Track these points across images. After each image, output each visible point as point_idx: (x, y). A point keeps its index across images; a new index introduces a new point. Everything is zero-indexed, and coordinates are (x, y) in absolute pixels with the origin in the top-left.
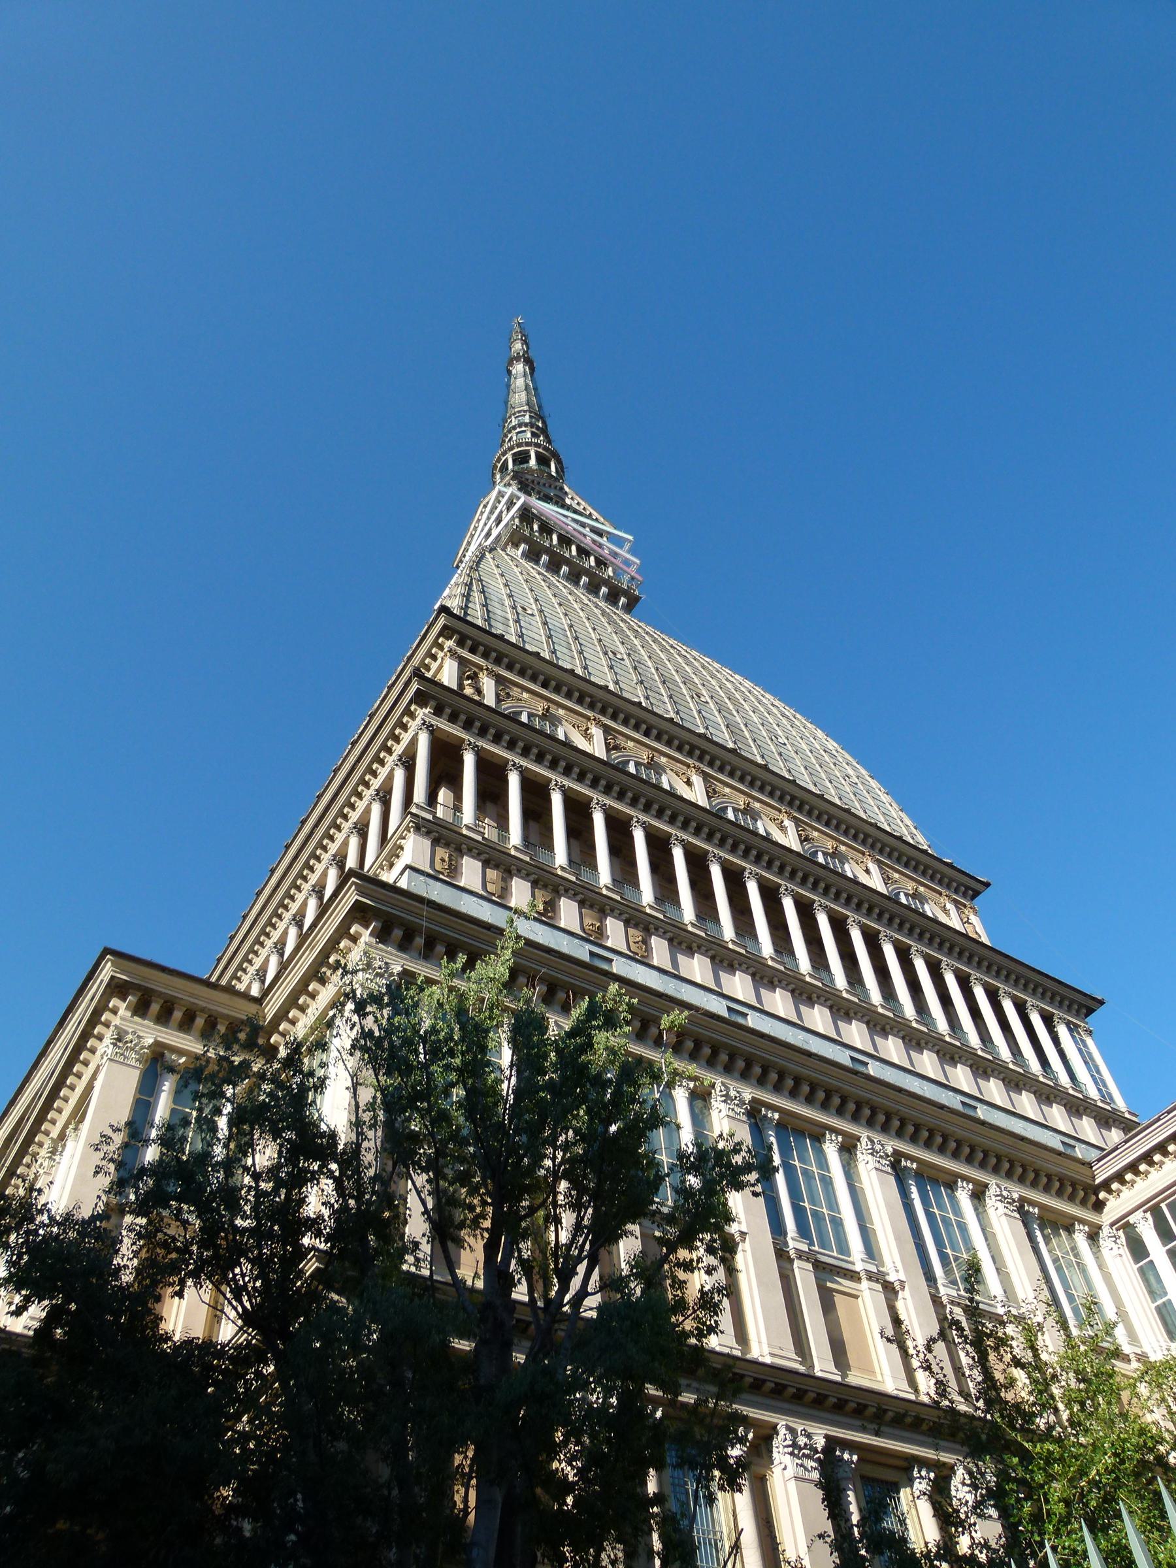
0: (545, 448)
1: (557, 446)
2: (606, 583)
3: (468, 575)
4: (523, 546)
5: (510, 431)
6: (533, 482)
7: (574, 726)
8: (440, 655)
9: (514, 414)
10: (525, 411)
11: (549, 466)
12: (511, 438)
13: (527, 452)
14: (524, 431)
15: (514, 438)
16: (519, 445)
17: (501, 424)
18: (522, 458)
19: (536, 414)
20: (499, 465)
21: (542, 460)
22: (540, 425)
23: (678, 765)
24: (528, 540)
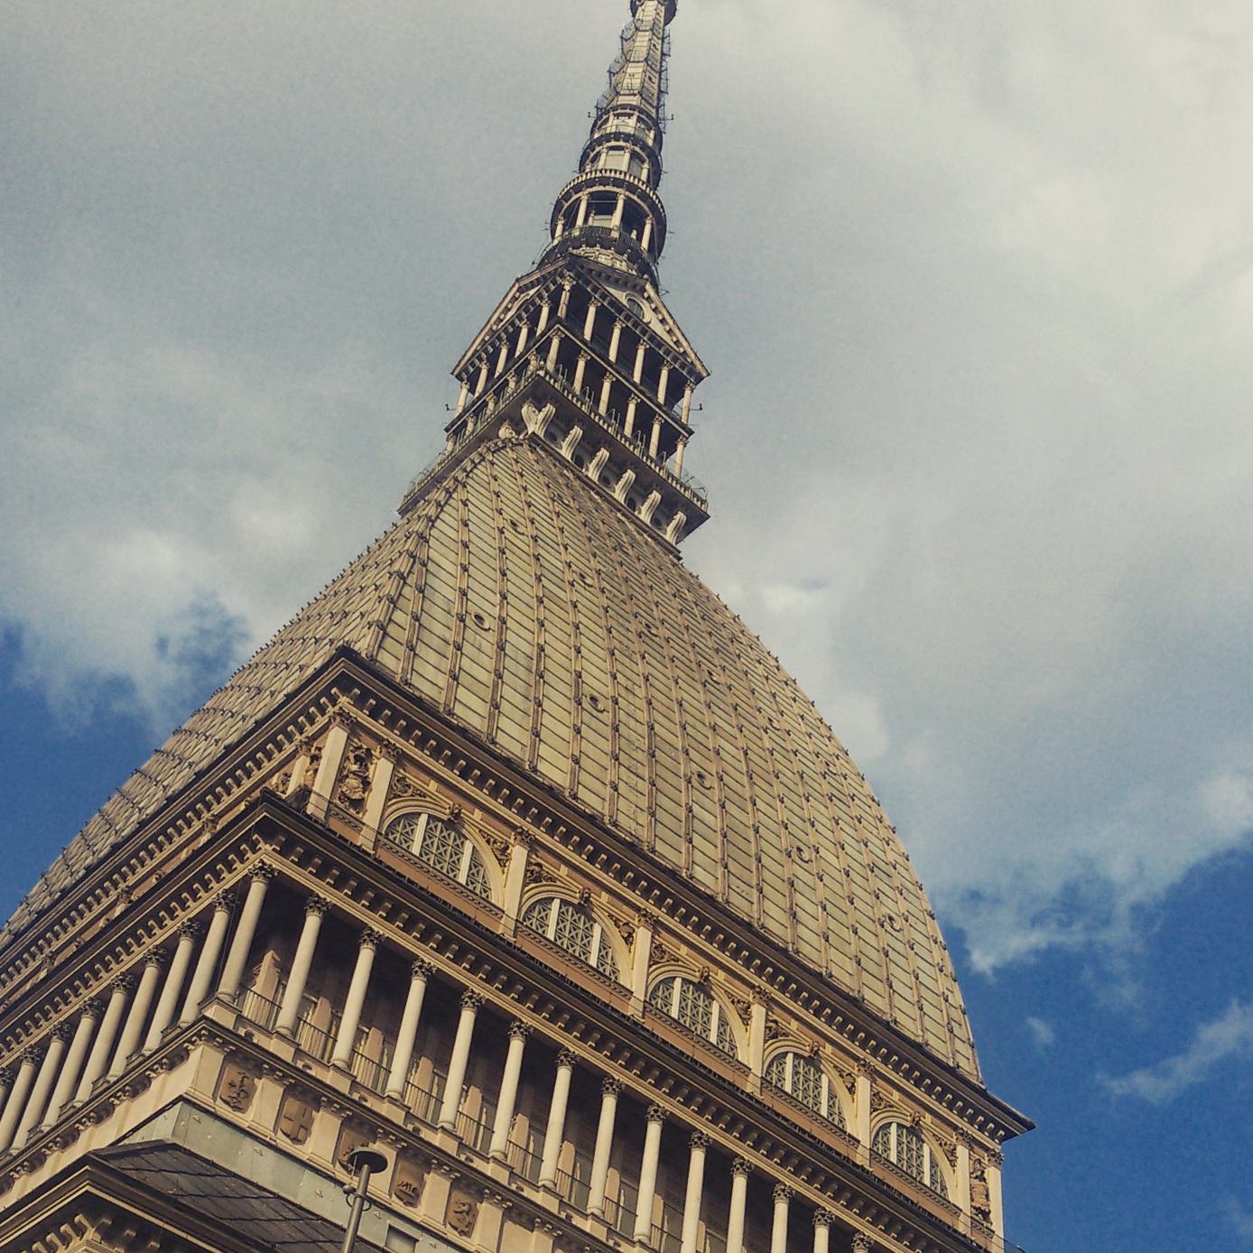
0: (644, 196)
1: (665, 193)
2: (661, 485)
3: (412, 556)
4: (549, 409)
5: (599, 142)
6: (599, 274)
7: (488, 842)
8: (331, 710)
9: (614, 109)
10: (633, 108)
11: (640, 237)
12: (599, 154)
13: (614, 196)
14: (621, 148)
15: (601, 164)
16: (604, 181)
17: (594, 113)
18: (602, 205)
19: (649, 116)
20: (566, 205)
21: (633, 219)
22: (650, 143)
23: (625, 908)
24: (557, 399)
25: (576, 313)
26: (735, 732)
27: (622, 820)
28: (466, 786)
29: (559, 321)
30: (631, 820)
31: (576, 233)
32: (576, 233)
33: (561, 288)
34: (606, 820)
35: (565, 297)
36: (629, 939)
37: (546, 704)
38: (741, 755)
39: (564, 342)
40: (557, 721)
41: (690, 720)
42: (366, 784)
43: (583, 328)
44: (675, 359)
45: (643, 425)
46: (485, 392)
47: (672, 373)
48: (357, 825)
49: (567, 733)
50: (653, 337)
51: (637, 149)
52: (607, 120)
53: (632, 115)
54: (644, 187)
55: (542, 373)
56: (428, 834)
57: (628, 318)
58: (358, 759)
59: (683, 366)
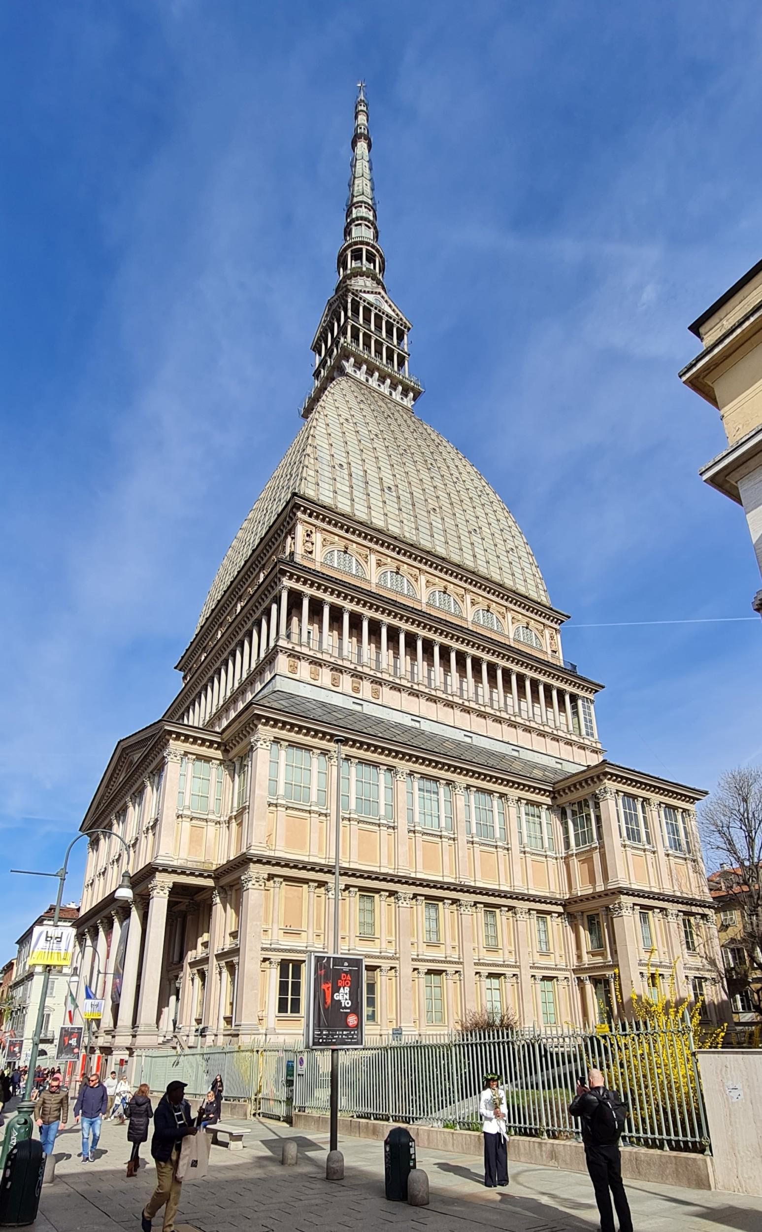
0: (373, 247)
4: (352, 360)
5: (350, 224)
6: (361, 291)
10: (362, 202)
13: (361, 249)
14: (360, 224)
16: (356, 243)
17: (346, 209)
19: (369, 205)
20: (342, 259)
22: (371, 218)
23: (414, 569)
25: (356, 311)
26: (443, 487)
27: (407, 535)
28: (348, 536)
29: (349, 318)
30: (410, 535)
31: (349, 272)
32: (349, 272)
33: (347, 302)
34: (401, 536)
35: (349, 305)
36: (416, 581)
37: (371, 494)
38: (446, 496)
39: (353, 326)
40: (376, 502)
41: (427, 486)
42: (313, 544)
43: (358, 318)
44: (398, 323)
45: (390, 358)
46: (325, 355)
47: (398, 328)
48: (313, 560)
49: (381, 505)
50: (387, 316)
51: (367, 223)
52: (352, 211)
53: (361, 206)
54: (372, 242)
55: (345, 344)
56: (339, 558)
57: (376, 308)
58: (308, 535)
59: (401, 325)
